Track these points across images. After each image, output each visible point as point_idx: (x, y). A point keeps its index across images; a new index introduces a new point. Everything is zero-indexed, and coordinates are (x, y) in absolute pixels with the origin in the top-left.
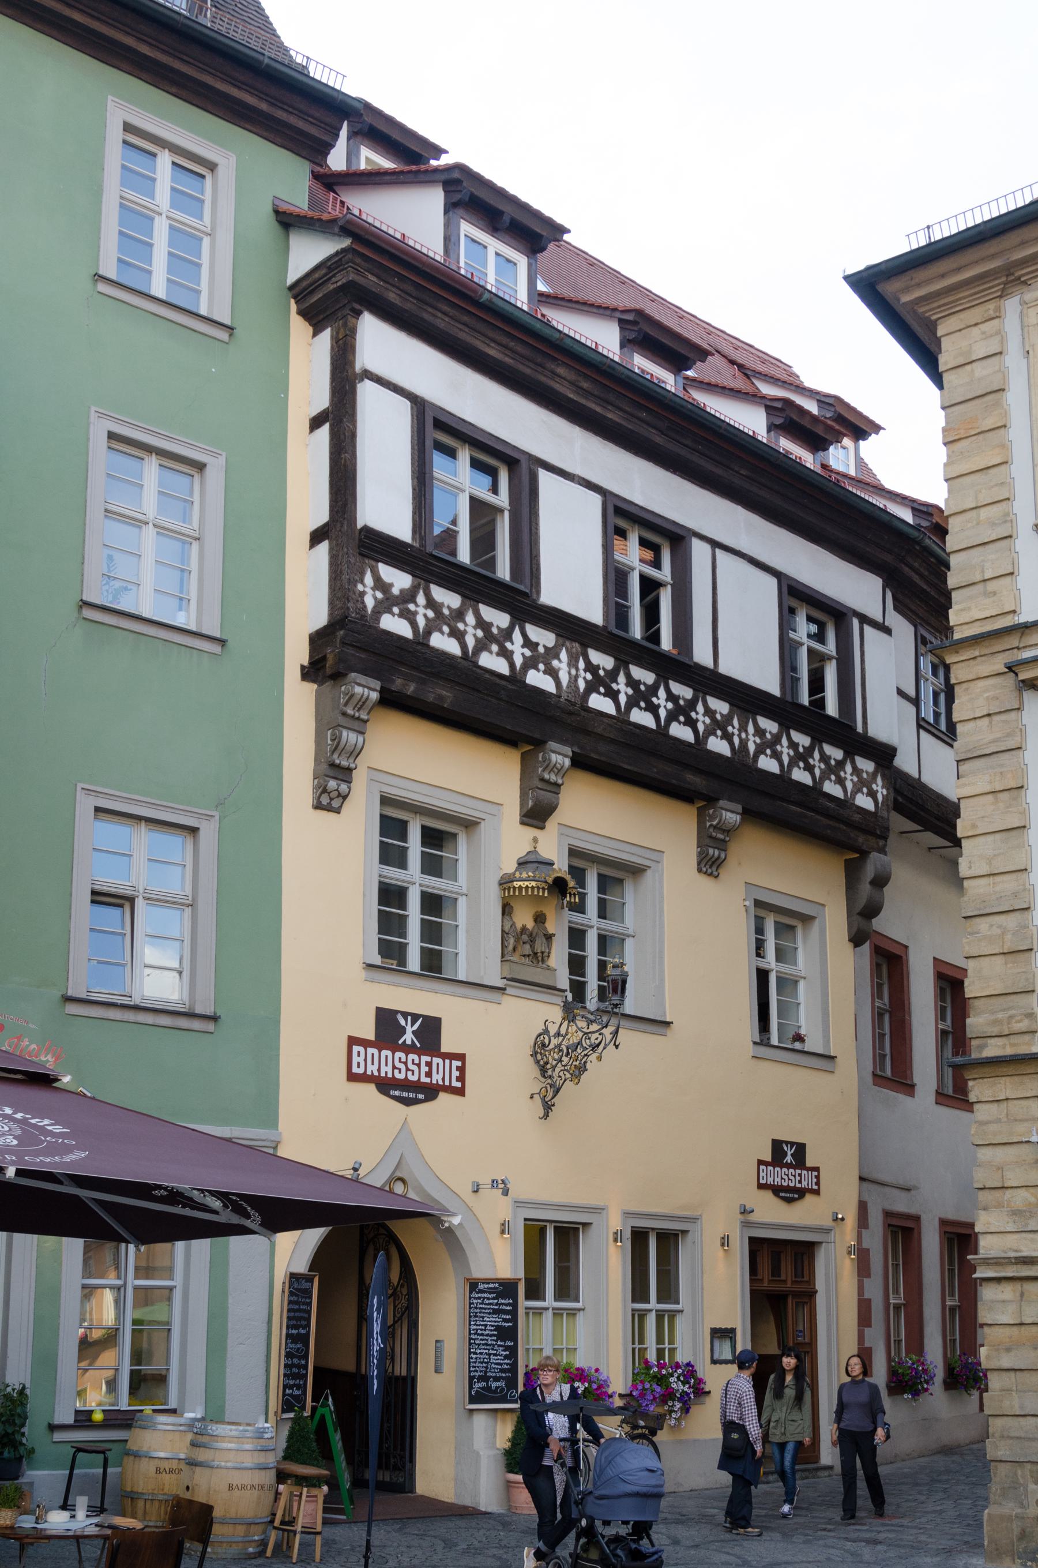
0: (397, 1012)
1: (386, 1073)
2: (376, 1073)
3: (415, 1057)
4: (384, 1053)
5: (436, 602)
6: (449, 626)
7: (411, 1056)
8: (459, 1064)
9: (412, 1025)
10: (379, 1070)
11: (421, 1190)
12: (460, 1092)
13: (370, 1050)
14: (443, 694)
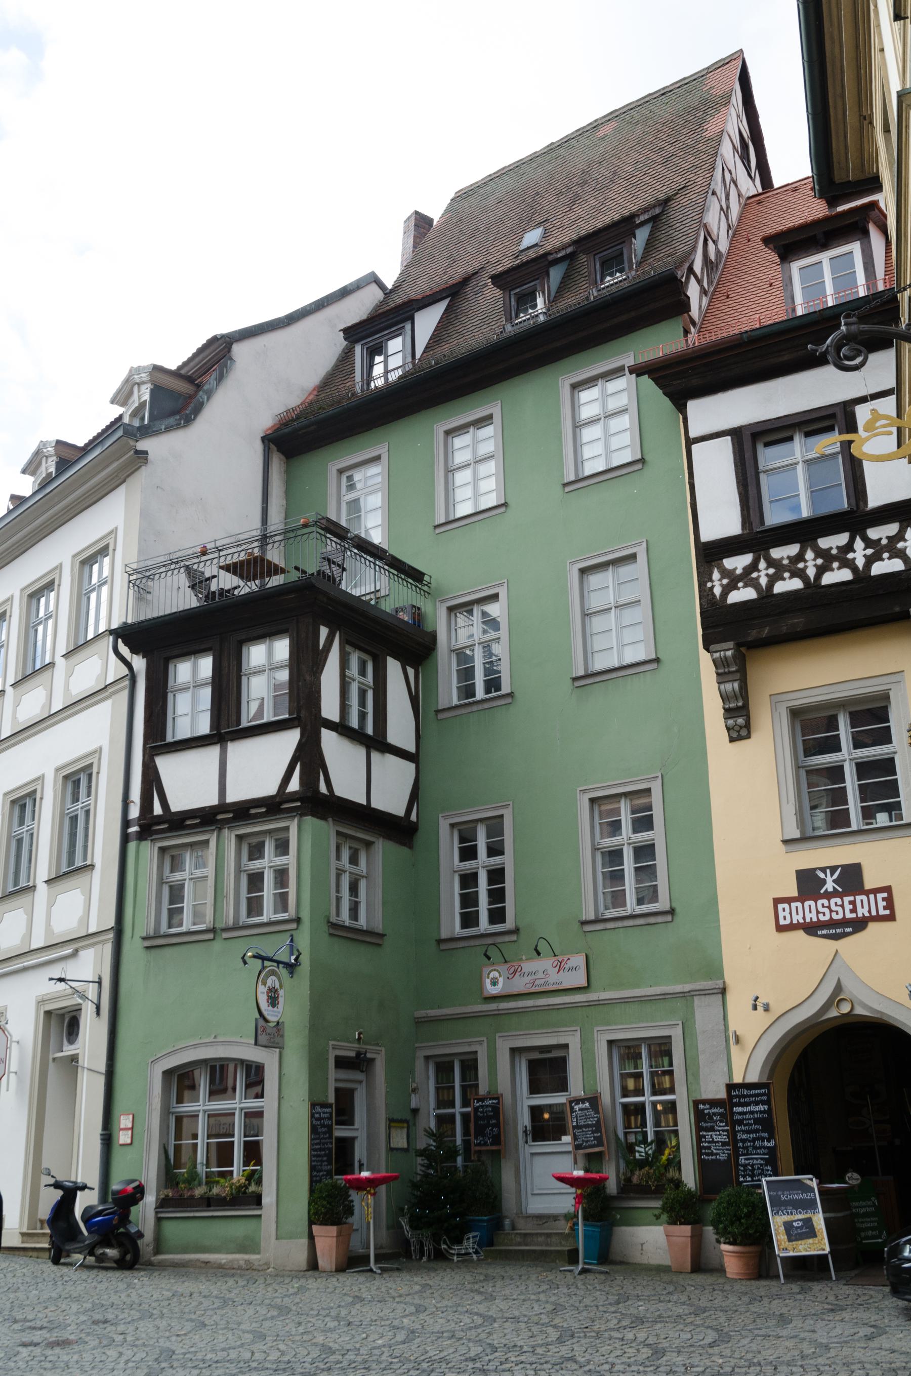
0: (815, 869)
1: (811, 918)
2: (801, 921)
3: (839, 901)
4: (807, 904)
5: (775, 560)
6: (789, 571)
7: (833, 901)
8: (885, 895)
9: (832, 876)
10: (804, 918)
11: (865, 1006)
12: (891, 918)
13: (794, 905)
14: (798, 621)
